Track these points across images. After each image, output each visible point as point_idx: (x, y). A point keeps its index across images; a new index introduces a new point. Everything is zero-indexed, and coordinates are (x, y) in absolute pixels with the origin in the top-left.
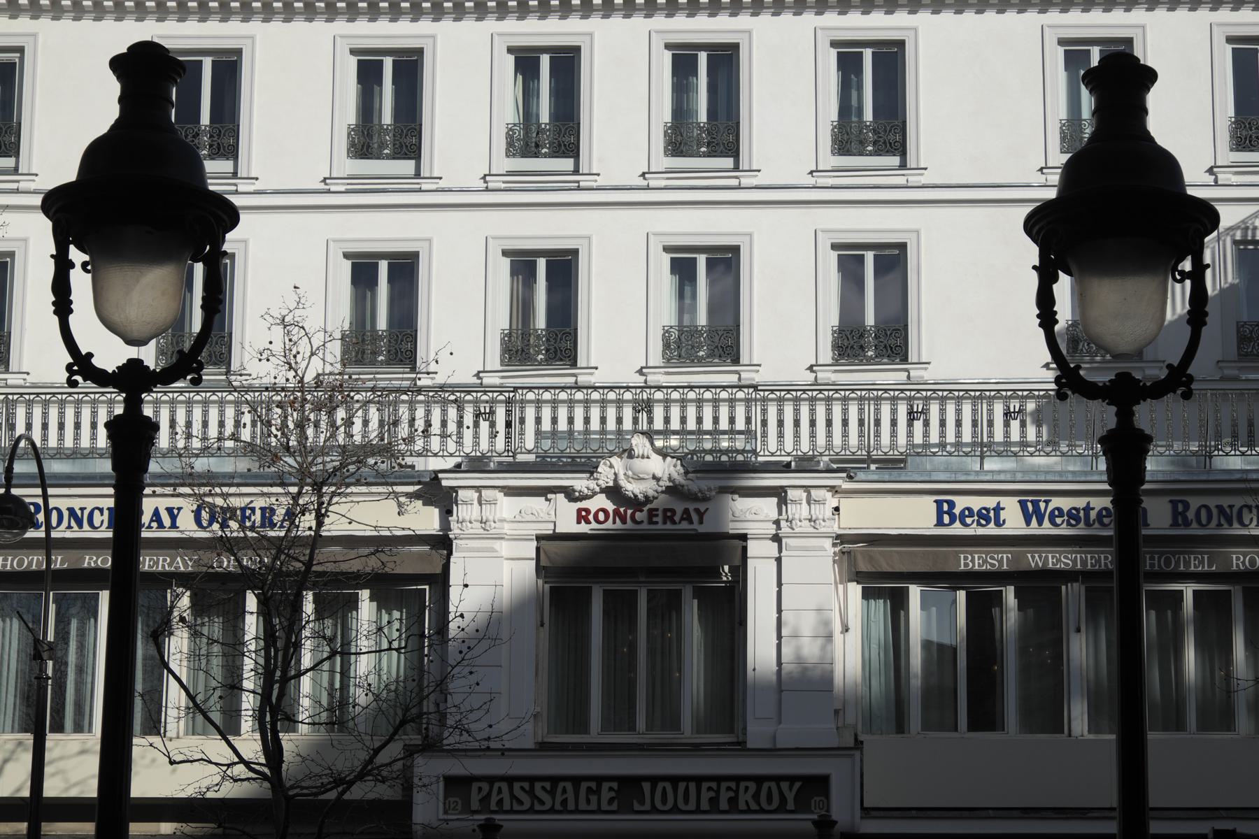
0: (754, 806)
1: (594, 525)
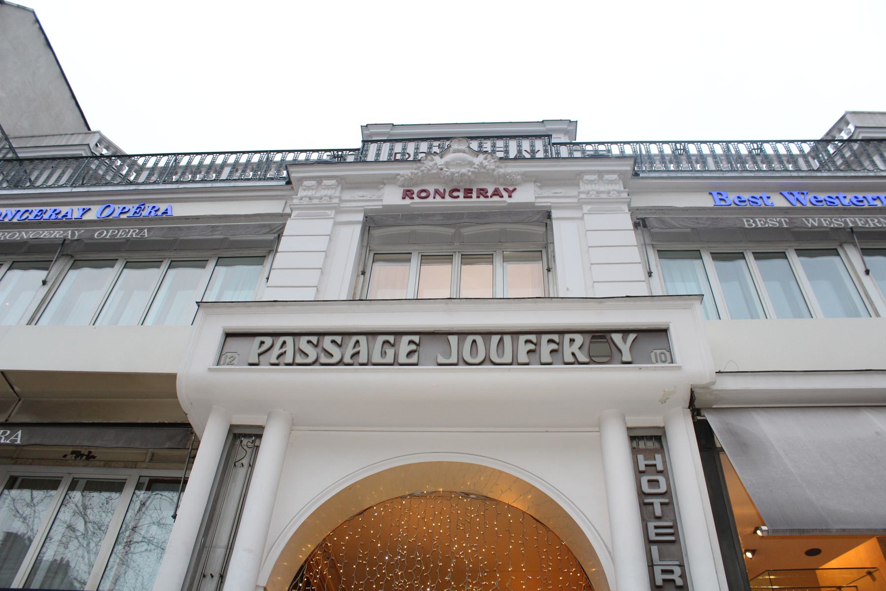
1: (417, 200)
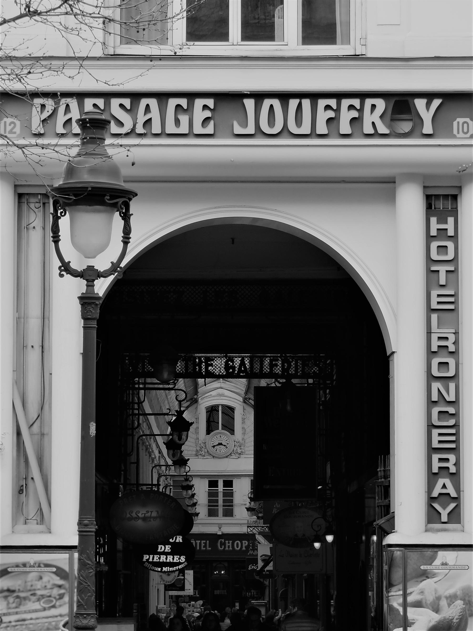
0: (382, 129)
